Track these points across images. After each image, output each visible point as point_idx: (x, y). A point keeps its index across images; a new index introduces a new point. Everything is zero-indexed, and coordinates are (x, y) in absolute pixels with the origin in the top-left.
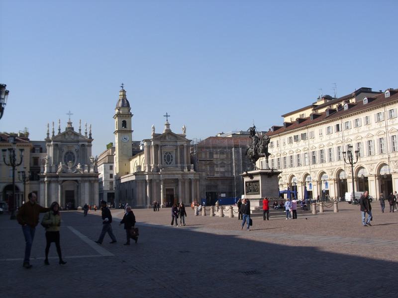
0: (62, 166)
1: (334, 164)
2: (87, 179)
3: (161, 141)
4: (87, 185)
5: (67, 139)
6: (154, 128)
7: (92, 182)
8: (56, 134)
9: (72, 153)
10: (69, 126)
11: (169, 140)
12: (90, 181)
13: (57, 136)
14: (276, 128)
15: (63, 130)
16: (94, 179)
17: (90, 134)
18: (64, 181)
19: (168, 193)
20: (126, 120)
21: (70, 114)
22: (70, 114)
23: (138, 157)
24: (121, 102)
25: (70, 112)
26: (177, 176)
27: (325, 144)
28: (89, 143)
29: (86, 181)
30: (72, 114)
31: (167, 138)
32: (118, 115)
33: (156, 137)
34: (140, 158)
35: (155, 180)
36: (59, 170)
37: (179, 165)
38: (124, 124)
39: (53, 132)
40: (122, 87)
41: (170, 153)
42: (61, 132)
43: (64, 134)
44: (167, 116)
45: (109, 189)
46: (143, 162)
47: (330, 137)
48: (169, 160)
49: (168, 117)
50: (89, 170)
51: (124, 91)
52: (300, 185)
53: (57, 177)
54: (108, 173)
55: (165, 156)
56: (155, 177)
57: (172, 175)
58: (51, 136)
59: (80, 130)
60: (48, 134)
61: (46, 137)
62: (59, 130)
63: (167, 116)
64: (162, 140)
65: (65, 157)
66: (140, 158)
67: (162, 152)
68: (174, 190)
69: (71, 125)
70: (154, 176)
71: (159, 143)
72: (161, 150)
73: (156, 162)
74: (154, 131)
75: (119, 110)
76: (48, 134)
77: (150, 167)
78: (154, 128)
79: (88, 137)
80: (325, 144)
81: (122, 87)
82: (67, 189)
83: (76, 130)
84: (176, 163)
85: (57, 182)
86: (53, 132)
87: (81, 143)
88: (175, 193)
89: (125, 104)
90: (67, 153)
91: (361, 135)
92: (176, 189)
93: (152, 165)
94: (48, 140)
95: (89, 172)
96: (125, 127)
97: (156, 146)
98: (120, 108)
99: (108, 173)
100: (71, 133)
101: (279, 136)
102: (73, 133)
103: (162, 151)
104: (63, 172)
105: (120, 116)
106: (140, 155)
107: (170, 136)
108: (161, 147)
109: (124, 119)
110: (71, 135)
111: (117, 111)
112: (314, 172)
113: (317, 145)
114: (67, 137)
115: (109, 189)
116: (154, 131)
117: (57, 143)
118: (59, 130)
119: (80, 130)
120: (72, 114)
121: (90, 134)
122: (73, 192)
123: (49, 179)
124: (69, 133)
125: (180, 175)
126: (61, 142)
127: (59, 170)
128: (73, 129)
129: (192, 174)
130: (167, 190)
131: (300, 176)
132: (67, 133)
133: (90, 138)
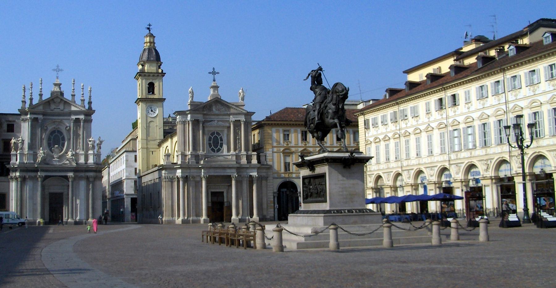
0: (44, 153)
1: (490, 151)
2: (82, 174)
3: (204, 115)
4: (83, 184)
5: (52, 110)
6: (192, 93)
7: (91, 180)
8: (35, 102)
9: (61, 133)
10: (57, 89)
11: (217, 112)
12: (87, 178)
13: (38, 105)
14: (393, 92)
15: (47, 96)
16: (91, 174)
17: (90, 103)
18: (46, 177)
19: (215, 199)
20: (153, 81)
21: (58, 70)
22: (58, 70)
23: (170, 140)
24: (146, 53)
25: (58, 66)
26: (228, 171)
27: (475, 115)
28: (89, 118)
29: (81, 178)
30: (61, 70)
31: (214, 110)
32: (141, 74)
33: (196, 108)
34: (172, 142)
35: (193, 177)
36: (39, 159)
37: (232, 152)
38: (151, 88)
39: (31, 99)
41: (218, 134)
42: (44, 98)
43: (48, 102)
44: (214, 73)
45: (133, 193)
46: (176, 149)
47: (483, 104)
49: (216, 76)
50: (86, 159)
51: (151, 36)
52: (459, 184)
53: (36, 170)
54: (132, 167)
56: (193, 172)
58: (27, 105)
59: (73, 96)
60: (24, 102)
61: (20, 106)
62: (41, 95)
63: (214, 73)
64: (205, 112)
65: (49, 139)
66: (172, 142)
67: (206, 132)
68: (225, 194)
69: (60, 88)
70: (192, 171)
71: (200, 117)
72: (203, 127)
73: (195, 148)
74: (192, 97)
75: (142, 65)
76: (24, 102)
77: (184, 156)
78: (192, 93)
79: (87, 107)
80: (475, 115)
81: (148, 29)
82: (52, 191)
83: (67, 96)
84: (229, 150)
85: (35, 179)
86: (31, 99)
87: (74, 117)
88: (225, 200)
89: (153, 55)
90: (53, 132)
91: (539, 98)
92: (227, 193)
93: (188, 153)
94: (23, 112)
95: (86, 163)
96: (153, 93)
97: (196, 123)
98: (144, 62)
99: (132, 167)
100: (59, 100)
101: (397, 104)
102: (61, 100)
103: (206, 129)
104: (44, 160)
105: (145, 75)
106: (172, 137)
107: (219, 106)
108: (203, 123)
109: (151, 81)
110: (60, 103)
111: (140, 67)
112: (457, 164)
113: (461, 119)
114: (53, 106)
115: (133, 193)
116: (192, 97)
117: (36, 116)
118: (41, 95)
119: (73, 96)
120: (61, 70)
121: (90, 103)
122: (61, 194)
123: (24, 174)
124: (55, 100)
125: (234, 170)
126: (44, 114)
127: (39, 159)
128: (62, 94)
129: (254, 168)
130: (213, 194)
131: (432, 172)
132: (53, 100)
133: (90, 108)
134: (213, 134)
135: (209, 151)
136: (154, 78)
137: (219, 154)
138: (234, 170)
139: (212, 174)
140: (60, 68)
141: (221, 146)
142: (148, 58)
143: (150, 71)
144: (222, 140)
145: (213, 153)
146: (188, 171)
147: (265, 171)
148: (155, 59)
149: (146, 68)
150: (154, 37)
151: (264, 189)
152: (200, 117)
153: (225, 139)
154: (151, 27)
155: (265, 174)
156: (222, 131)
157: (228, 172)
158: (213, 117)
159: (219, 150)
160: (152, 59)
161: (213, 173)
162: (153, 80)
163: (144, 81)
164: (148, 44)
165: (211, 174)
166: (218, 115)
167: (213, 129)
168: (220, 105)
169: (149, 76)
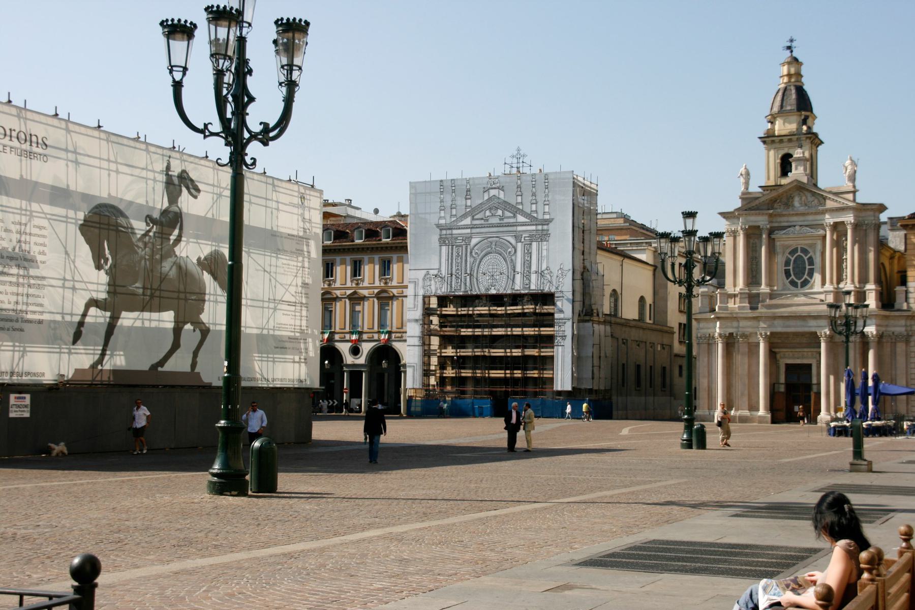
3: (771, 215)
20: (791, 152)
26: (812, 323)
31: (796, 203)
40: (789, 48)
41: (805, 251)
48: (799, 274)
55: (787, 263)
56: (746, 326)
57: (799, 323)
70: (743, 323)
71: (762, 220)
81: (789, 48)
84: (823, 283)
97: (752, 234)
103: (778, 244)
105: (773, 142)
116: (747, 184)
134: (794, 251)
135: (784, 285)
136: (791, 144)
137: (806, 290)
138: (824, 322)
139: (779, 330)
140: (522, 152)
141: (811, 274)
142: (782, 106)
143: (783, 133)
144: (811, 262)
145: (794, 290)
146: (735, 324)
147: (903, 322)
148: (794, 107)
149: (777, 127)
150: (801, 64)
151: (901, 360)
152: (762, 220)
153: (817, 260)
154: (794, 44)
155: (903, 329)
156: (813, 246)
157: (811, 326)
158: (795, 218)
159: (805, 283)
160: (789, 108)
161: (779, 327)
162: (790, 148)
163: (772, 153)
164: (786, 79)
165: (775, 330)
166: (803, 214)
167: (793, 244)
168: (809, 195)
169: (781, 141)
